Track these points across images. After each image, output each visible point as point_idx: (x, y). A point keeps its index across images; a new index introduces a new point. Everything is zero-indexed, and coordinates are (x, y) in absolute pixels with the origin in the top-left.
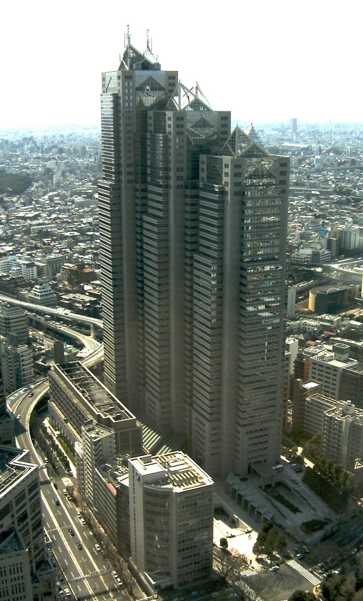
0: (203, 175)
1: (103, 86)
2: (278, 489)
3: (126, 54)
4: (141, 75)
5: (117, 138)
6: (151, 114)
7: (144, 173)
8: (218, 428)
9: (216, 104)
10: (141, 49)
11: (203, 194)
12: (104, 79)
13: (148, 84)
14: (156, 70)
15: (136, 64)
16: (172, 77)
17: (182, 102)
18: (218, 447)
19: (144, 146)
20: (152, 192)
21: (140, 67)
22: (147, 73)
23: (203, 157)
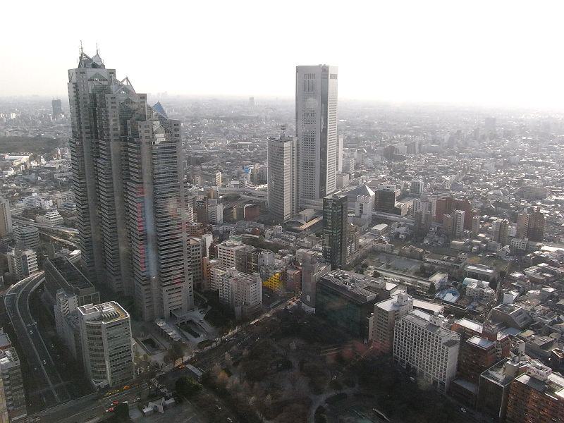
0: (130, 132)
1: (69, 77)
2: (189, 325)
3: (81, 58)
4: (91, 72)
5: (79, 111)
6: (98, 95)
7: (96, 133)
8: (149, 289)
9: (138, 89)
10: (91, 54)
11: (129, 144)
12: (69, 74)
13: (97, 77)
14: (100, 67)
15: (89, 65)
16: (112, 72)
17: (113, 87)
18: (150, 302)
19: (95, 115)
20: (102, 145)
21: (91, 66)
22: (95, 70)
23: (129, 122)
